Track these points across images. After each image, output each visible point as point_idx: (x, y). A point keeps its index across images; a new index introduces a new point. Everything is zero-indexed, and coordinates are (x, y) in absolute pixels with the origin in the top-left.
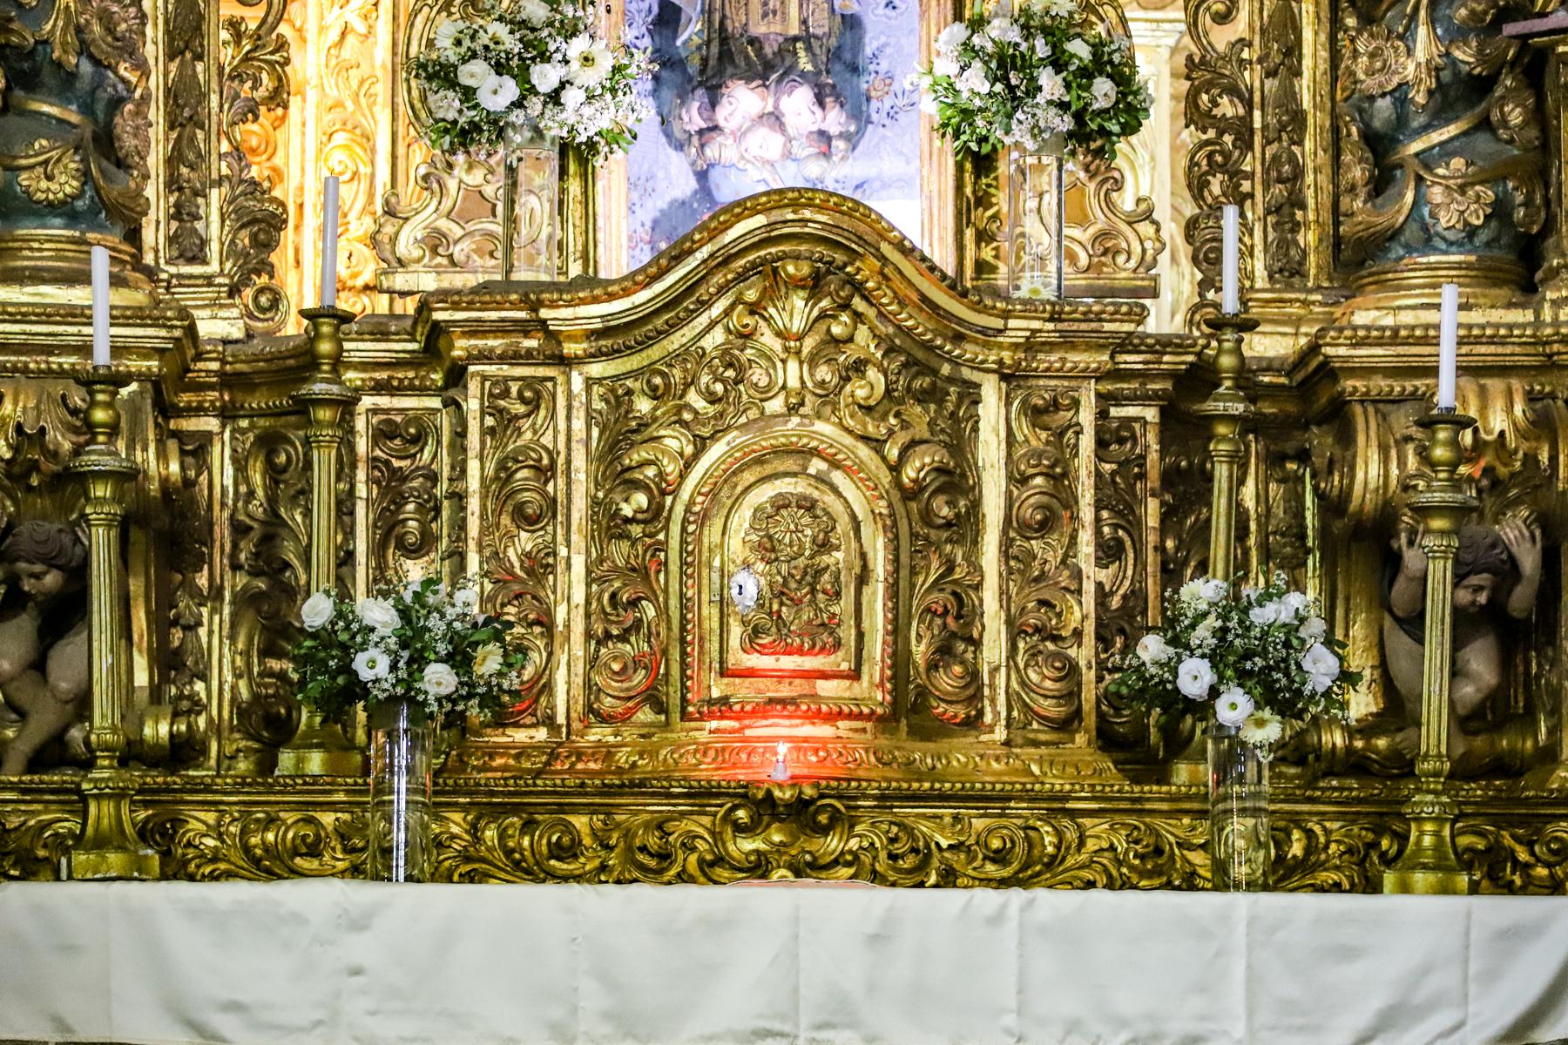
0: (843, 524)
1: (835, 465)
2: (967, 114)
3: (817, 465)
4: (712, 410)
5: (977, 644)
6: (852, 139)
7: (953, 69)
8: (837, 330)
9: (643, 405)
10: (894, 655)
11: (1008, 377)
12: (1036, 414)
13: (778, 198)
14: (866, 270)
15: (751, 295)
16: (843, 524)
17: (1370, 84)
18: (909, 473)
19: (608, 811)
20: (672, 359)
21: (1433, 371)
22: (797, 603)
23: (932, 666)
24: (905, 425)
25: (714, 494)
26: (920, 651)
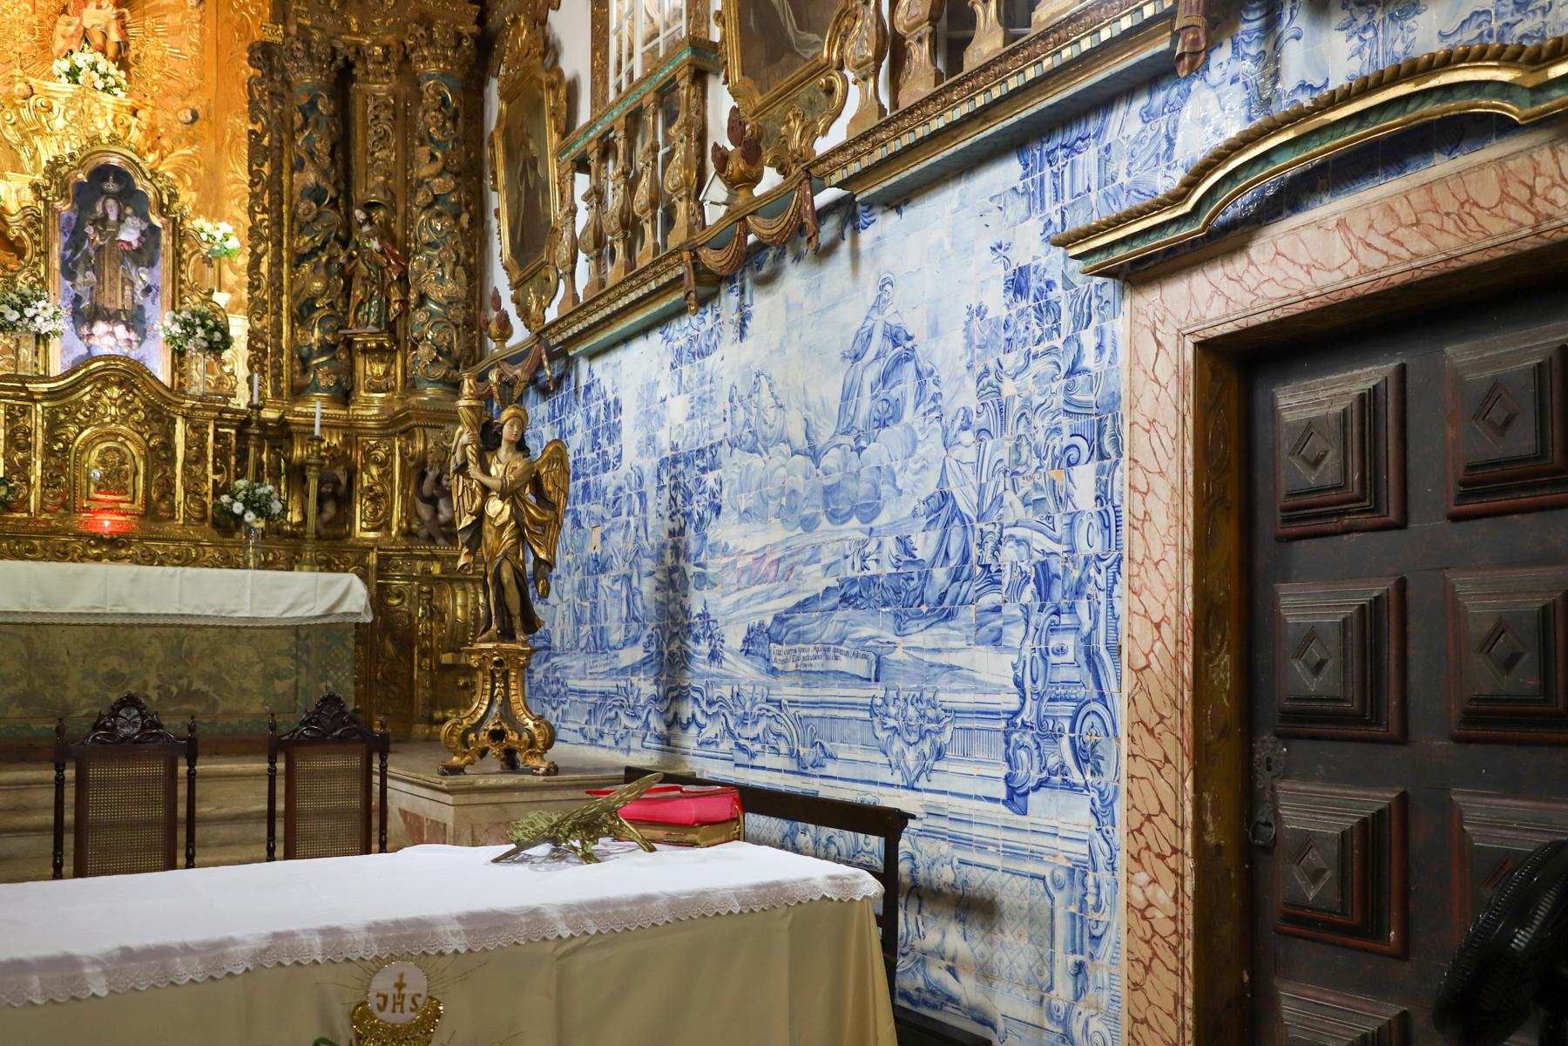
0: (129, 457)
1: (127, 439)
2: (174, 338)
3: (121, 439)
6: (140, 343)
9: (62, 417)
11: (186, 417)
12: (194, 429)
13: (114, 357)
16: (129, 457)
18: (152, 443)
19: (46, 539)
20: (72, 403)
21: (314, 426)
22: (113, 480)
23: (159, 501)
25: (86, 445)
26: (155, 496)
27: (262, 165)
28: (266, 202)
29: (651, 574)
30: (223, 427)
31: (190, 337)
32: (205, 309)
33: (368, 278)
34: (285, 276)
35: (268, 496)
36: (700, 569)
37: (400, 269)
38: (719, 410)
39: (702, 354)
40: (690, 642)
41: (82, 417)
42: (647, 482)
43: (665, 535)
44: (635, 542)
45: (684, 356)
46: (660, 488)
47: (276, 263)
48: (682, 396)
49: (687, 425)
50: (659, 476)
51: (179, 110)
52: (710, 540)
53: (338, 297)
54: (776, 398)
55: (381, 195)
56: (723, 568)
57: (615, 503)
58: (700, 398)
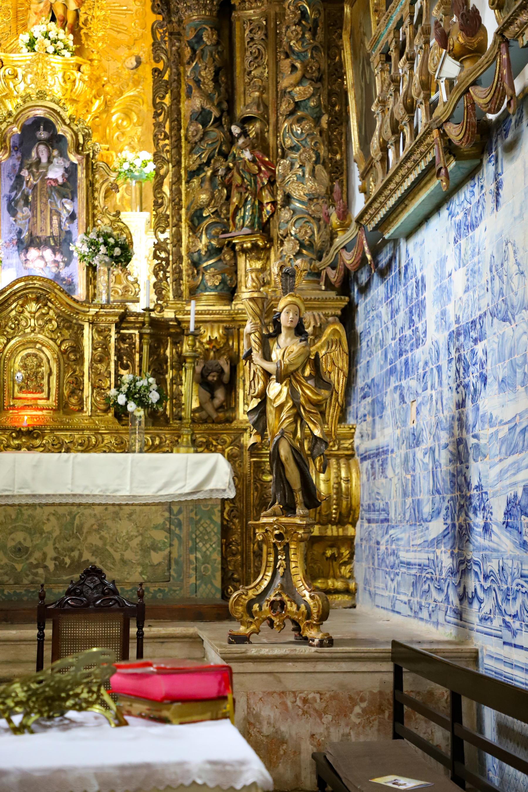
1: (43, 345)
2: (84, 256)
3: (38, 346)
4: (12, 331)
5: (82, 390)
7: (80, 245)
8: (44, 311)
10: (59, 394)
11: (92, 323)
12: (99, 332)
14: (52, 297)
15: (20, 302)
16: (45, 360)
17: (192, 250)
18: (63, 348)
22: (32, 380)
23: (69, 396)
24: (62, 335)
25: (12, 353)
26: (66, 392)
27: (164, 97)
28: (167, 130)
30: (127, 328)
31: (96, 254)
32: (109, 230)
33: (241, 186)
34: (183, 192)
35: (148, 387)
37: (269, 174)
41: (9, 330)
47: (177, 180)
51: (126, 58)
53: (222, 205)
55: (254, 109)
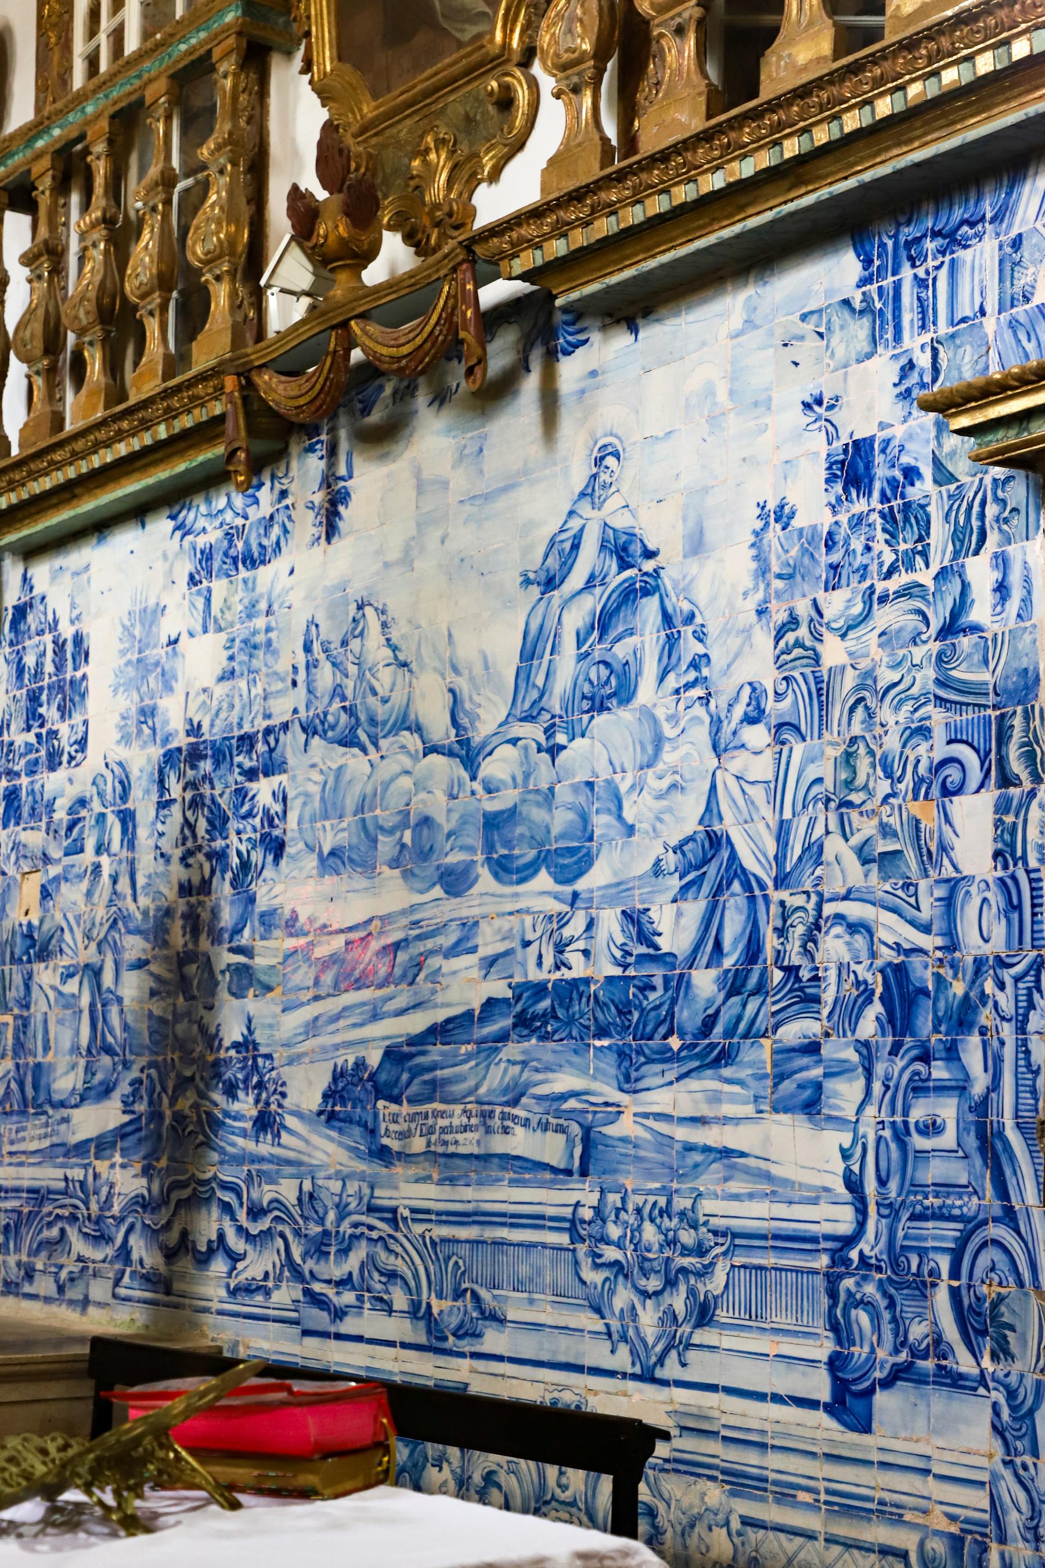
29: (140, 965)
36: (241, 959)
38: (283, 666)
39: (252, 561)
40: (217, 1096)
42: (136, 792)
43: (170, 892)
44: (111, 903)
45: (216, 564)
46: (164, 805)
48: (210, 636)
49: (220, 691)
50: (161, 782)
52: (262, 904)
54: (395, 649)
56: (287, 957)
57: (70, 828)
58: (245, 642)
